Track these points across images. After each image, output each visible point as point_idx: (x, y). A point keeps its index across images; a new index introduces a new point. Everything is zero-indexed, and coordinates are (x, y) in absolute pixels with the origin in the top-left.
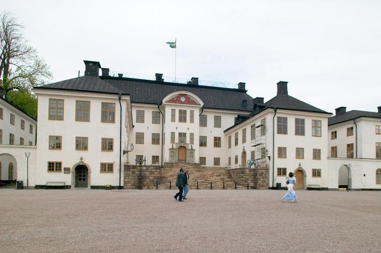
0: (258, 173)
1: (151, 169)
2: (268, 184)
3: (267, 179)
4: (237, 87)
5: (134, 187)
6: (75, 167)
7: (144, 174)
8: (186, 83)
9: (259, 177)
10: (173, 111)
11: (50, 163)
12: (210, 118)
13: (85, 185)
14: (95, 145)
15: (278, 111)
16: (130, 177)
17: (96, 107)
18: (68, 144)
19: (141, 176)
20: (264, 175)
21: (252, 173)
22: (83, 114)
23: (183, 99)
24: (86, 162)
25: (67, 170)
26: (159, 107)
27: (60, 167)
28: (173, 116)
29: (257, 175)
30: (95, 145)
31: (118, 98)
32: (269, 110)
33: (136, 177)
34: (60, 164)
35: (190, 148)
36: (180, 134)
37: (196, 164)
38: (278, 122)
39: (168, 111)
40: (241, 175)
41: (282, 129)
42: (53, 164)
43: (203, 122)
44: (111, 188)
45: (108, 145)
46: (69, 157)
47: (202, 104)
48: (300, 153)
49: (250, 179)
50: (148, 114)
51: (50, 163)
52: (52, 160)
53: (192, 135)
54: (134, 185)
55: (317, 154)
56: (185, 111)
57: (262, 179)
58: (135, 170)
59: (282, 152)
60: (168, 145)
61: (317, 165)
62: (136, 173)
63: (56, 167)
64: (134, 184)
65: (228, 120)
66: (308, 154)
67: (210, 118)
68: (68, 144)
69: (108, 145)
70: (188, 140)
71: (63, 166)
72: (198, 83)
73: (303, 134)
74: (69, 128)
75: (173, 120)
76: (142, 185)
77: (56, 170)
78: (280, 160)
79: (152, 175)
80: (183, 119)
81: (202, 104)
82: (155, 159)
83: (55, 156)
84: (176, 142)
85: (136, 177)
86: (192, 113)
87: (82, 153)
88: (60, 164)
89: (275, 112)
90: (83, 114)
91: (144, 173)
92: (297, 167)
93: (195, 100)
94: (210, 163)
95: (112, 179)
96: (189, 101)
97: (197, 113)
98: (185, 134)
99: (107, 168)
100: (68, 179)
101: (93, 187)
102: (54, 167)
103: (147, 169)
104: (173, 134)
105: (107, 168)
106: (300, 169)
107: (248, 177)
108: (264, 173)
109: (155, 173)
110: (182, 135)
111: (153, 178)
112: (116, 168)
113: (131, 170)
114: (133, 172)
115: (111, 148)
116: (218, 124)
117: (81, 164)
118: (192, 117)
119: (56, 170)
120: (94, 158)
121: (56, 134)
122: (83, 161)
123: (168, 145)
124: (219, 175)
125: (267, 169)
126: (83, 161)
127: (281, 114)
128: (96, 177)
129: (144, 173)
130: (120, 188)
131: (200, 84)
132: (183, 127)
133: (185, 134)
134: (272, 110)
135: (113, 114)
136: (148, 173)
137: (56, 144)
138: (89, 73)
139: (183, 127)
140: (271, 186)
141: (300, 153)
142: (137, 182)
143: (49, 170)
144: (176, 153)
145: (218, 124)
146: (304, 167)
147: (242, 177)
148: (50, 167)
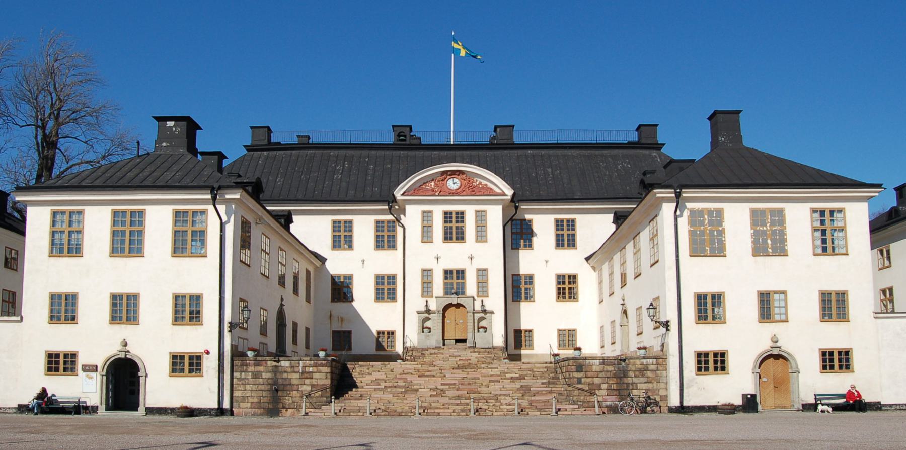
0: (631, 367)
1: (304, 367)
2: (665, 398)
3: (662, 385)
4: (634, 138)
5: (259, 411)
6: (140, 366)
7: (286, 379)
8: (485, 139)
9: (635, 380)
10: (427, 216)
11: (50, 355)
13: (134, 407)
14: (156, 310)
15: (687, 194)
16: (248, 387)
18: (94, 309)
19: (275, 382)
20: (649, 374)
21: (610, 368)
22: (127, 240)
24: (136, 351)
25: (88, 369)
26: (390, 209)
27: (74, 363)
29: (626, 376)
30: (156, 310)
31: (209, 197)
32: (660, 193)
33: (263, 387)
34: (74, 355)
35: (478, 307)
36: (448, 273)
37: (494, 348)
38: (692, 222)
39: (412, 216)
40: (577, 375)
41: (708, 242)
42: (58, 356)
44: (190, 412)
45: (187, 310)
46: (96, 340)
47: (509, 192)
48: (124, 308)
49: (604, 386)
50: (364, 226)
51: (50, 355)
52: (179, 349)
53: (482, 273)
54: (259, 405)
55: (833, 306)
56: (461, 216)
57: (645, 386)
58: (261, 369)
59: (709, 307)
60: (416, 302)
61: (835, 336)
62: (264, 375)
63: (65, 363)
64: (259, 402)
65: (594, 227)
66: (804, 307)
68: (94, 309)
70: (471, 287)
71: (81, 361)
72: (512, 138)
73: (780, 250)
74: (95, 274)
76: (281, 405)
77: (65, 370)
78: (707, 329)
79: (307, 381)
81: (509, 192)
83: (62, 339)
84: (435, 295)
85: (263, 387)
86: (481, 217)
87: (124, 331)
88: (74, 355)
89: (678, 196)
90: (127, 240)
91: (285, 375)
92: (765, 346)
93: (484, 182)
94: (544, 345)
95: (201, 391)
96: (472, 189)
97: (495, 216)
98: (461, 273)
99: (185, 364)
100: (88, 388)
101: (150, 411)
102: (61, 363)
103: (292, 367)
104: (427, 274)
105: (185, 364)
106: (776, 352)
107: (597, 381)
108: (652, 367)
109: (316, 376)
110: (454, 277)
111: (309, 388)
112: (210, 364)
113: (251, 369)
114: (256, 375)
115: (195, 316)
116: (566, 237)
117: (122, 356)
119: (65, 370)
120: (153, 342)
121: (65, 288)
122: (128, 348)
124: (521, 378)
125: (661, 359)
126: (128, 348)
127: (699, 201)
128: (160, 388)
129: (285, 375)
130: (221, 411)
131: (518, 139)
132: (454, 256)
133: (461, 273)
134: (669, 194)
135: (200, 236)
136: (297, 376)
137: (64, 308)
138: (164, 144)
139: (454, 256)
140: (675, 402)
141: (124, 308)
142: (265, 400)
143: (49, 370)
144: (435, 322)
145: (566, 237)
146: (787, 346)
147: (579, 382)
148: (50, 363)
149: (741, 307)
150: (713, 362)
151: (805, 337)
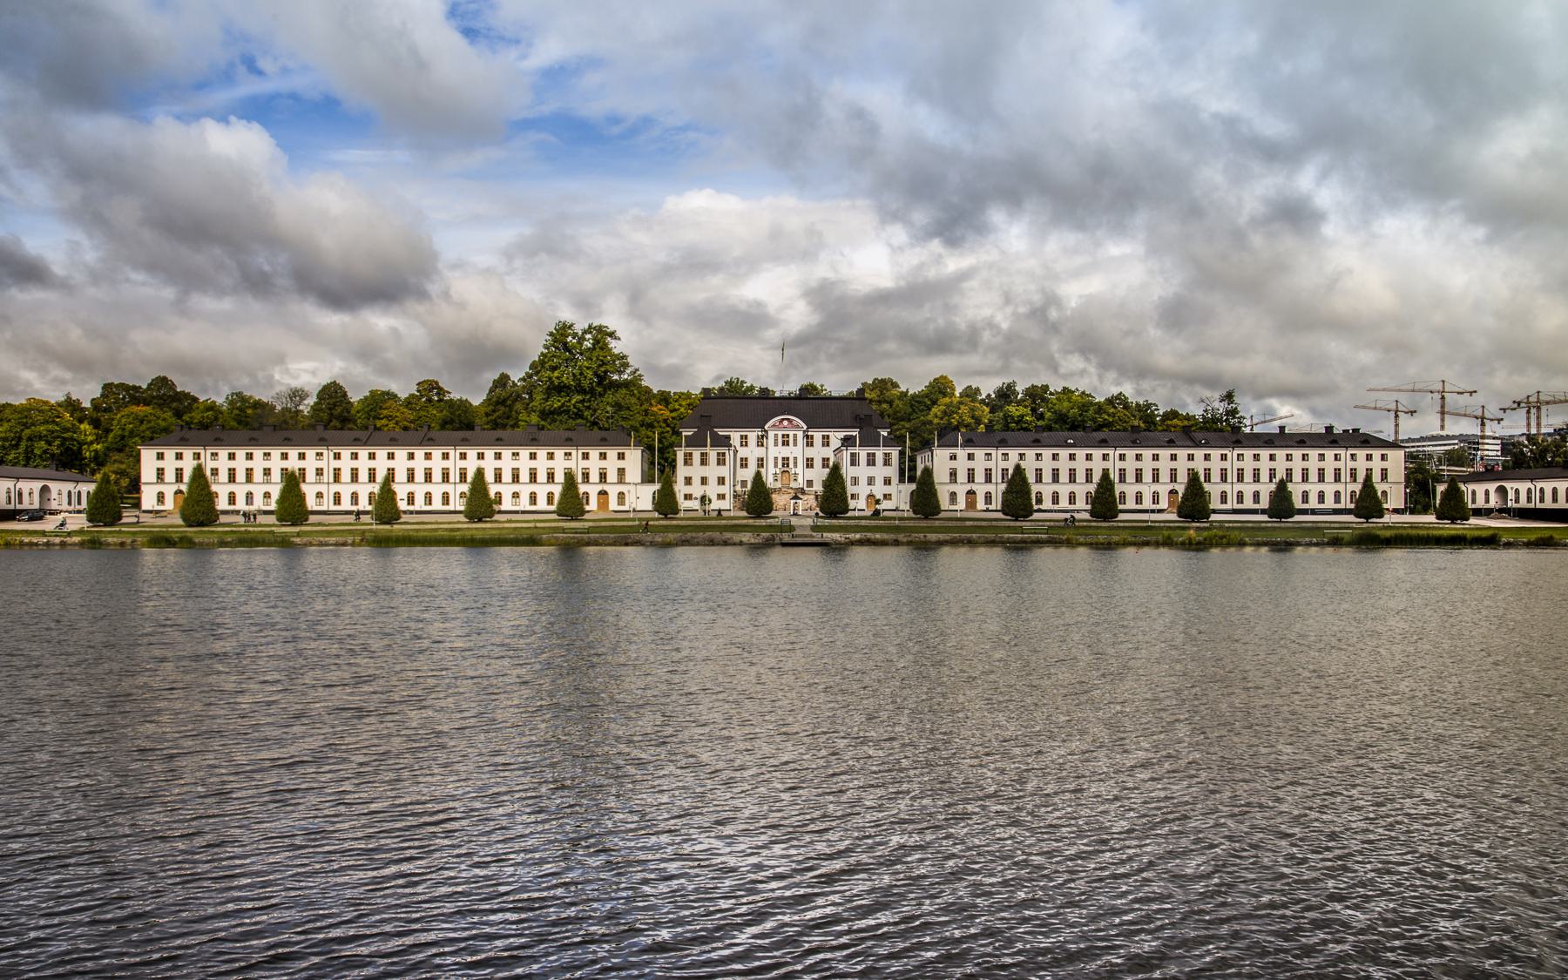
12: (817, 435)
14: (713, 481)
17: (713, 454)
18: (696, 481)
30: (713, 481)
39: (771, 434)
43: (810, 442)
45: (721, 481)
68: (696, 481)
69: (721, 481)
75: (776, 444)
80: (786, 443)
97: (800, 434)
99: (721, 497)
105: (721, 497)
110: (786, 460)
120: (712, 490)
145: (826, 442)
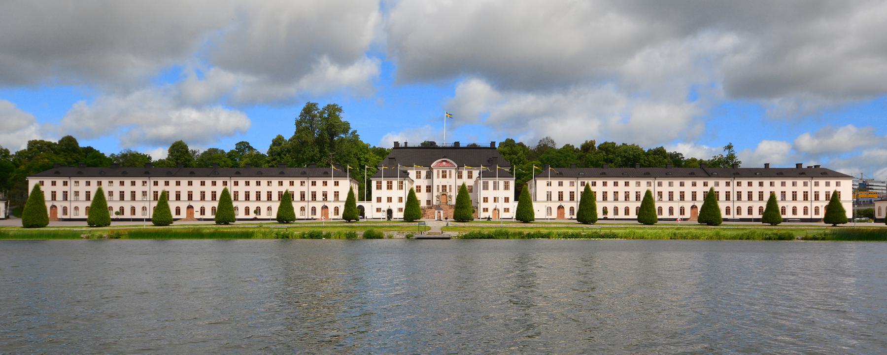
18: (384, 200)
23: (444, 163)
28: (438, 174)
39: (435, 172)
46: (385, 205)
50: (424, 173)
67: (465, 173)
68: (384, 200)
70: (448, 190)
74: (384, 193)
75: (438, 177)
80: (444, 176)
82: (429, 202)
83: (379, 205)
97: (453, 171)
110: (444, 187)
118: (450, 174)
123: (435, 193)
132: (444, 182)
137: (379, 200)
139: (444, 182)
149: (491, 200)
150: (486, 210)
151: (501, 205)
